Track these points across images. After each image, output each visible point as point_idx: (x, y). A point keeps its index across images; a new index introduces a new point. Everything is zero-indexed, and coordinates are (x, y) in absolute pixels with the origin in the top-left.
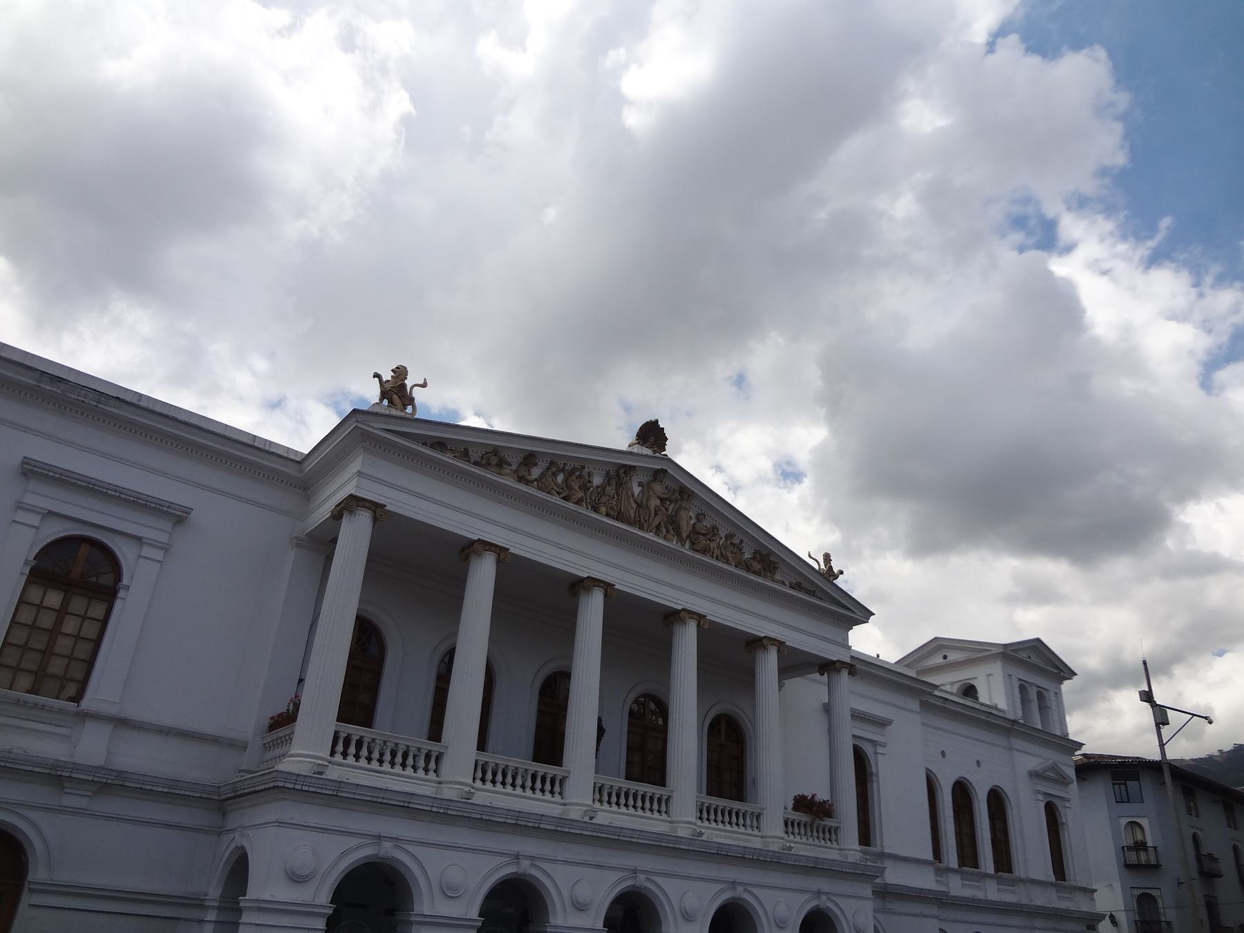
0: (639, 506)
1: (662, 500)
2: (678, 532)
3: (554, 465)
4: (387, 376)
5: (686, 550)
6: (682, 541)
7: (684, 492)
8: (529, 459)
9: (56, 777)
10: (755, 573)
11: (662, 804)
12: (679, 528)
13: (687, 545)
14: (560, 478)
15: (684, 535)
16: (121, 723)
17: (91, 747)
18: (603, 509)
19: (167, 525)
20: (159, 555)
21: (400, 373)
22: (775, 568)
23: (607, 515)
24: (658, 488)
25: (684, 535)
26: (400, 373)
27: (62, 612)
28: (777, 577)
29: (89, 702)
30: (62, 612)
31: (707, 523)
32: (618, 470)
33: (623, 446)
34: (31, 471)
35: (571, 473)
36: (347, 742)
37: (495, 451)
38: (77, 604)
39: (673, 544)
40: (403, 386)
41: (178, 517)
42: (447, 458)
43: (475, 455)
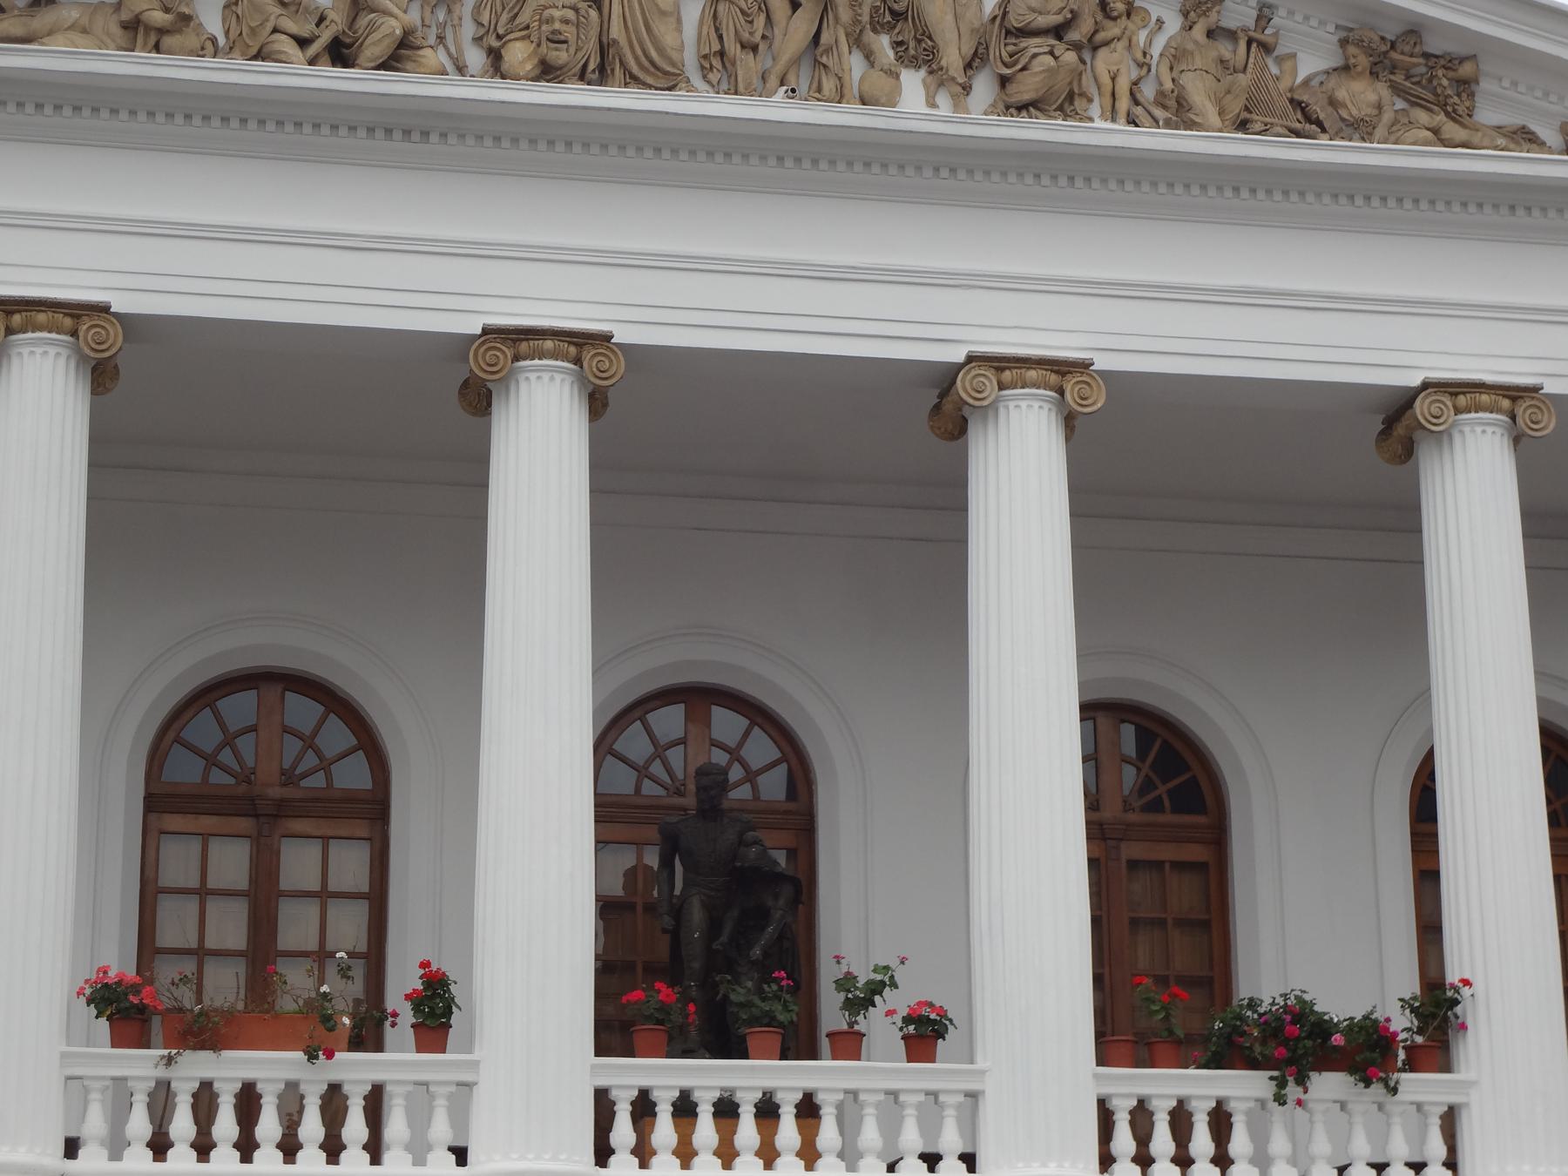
2: (920, 51)
5: (978, 120)
6: (938, 77)
10: (1361, 128)
12: (924, 34)
13: (984, 88)
15: (952, 58)
18: (518, 53)
22: (1465, 86)
23: (547, 72)
25: (952, 58)
27: (263, 897)
28: (1487, 115)
30: (263, 897)
36: (644, 1108)
38: (299, 863)
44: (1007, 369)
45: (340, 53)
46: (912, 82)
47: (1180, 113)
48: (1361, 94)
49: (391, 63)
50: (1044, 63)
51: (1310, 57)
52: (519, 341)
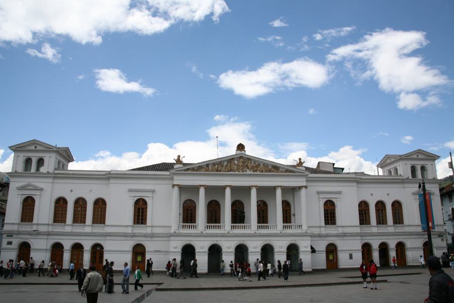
0: (237, 166)
1: (243, 163)
3: (214, 164)
4: (176, 158)
5: (252, 173)
6: (250, 170)
7: (249, 159)
8: (207, 165)
9: (146, 236)
10: (272, 172)
11: (250, 227)
14: (216, 166)
16: (152, 227)
17: (149, 231)
19: (151, 193)
20: (151, 198)
21: (179, 157)
23: (228, 171)
24: (241, 160)
26: (179, 157)
28: (280, 170)
29: (148, 224)
31: (257, 163)
32: (230, 160)
33: (234, 154)
34: (130, 191)
35: (218, 165)
37: (200, 166)
39: (248, 172)
40: (179, 160)
41: (153, 191)
42: (189, 172)
43: (196, 169)
44: (253, 186)
45: (217, 171)
46: (248, 170)
47: (263, 172)
48: (273, 169)
49: (220, 171)
50: (255, 169)
51: (270, 167)
52: (227, 186)
